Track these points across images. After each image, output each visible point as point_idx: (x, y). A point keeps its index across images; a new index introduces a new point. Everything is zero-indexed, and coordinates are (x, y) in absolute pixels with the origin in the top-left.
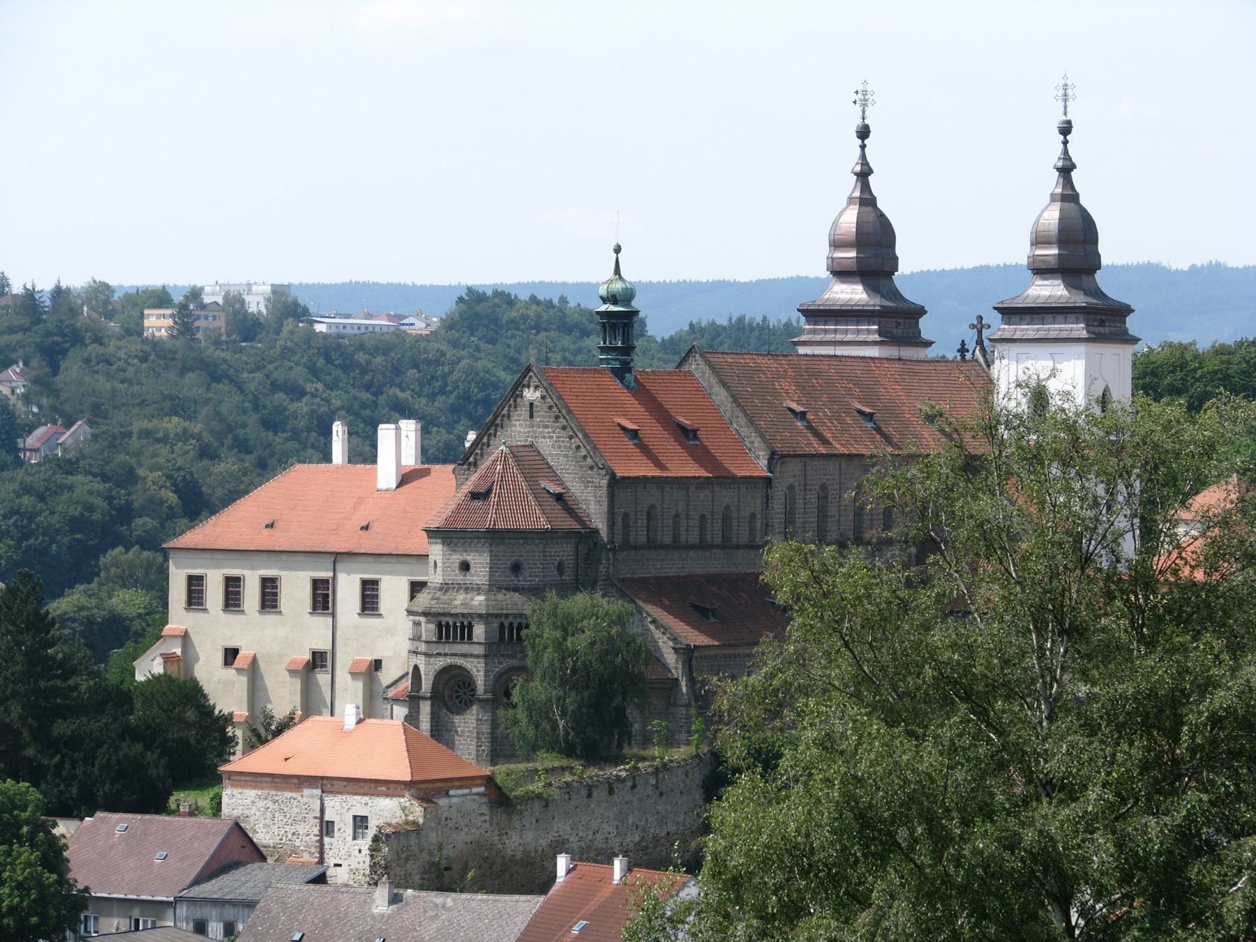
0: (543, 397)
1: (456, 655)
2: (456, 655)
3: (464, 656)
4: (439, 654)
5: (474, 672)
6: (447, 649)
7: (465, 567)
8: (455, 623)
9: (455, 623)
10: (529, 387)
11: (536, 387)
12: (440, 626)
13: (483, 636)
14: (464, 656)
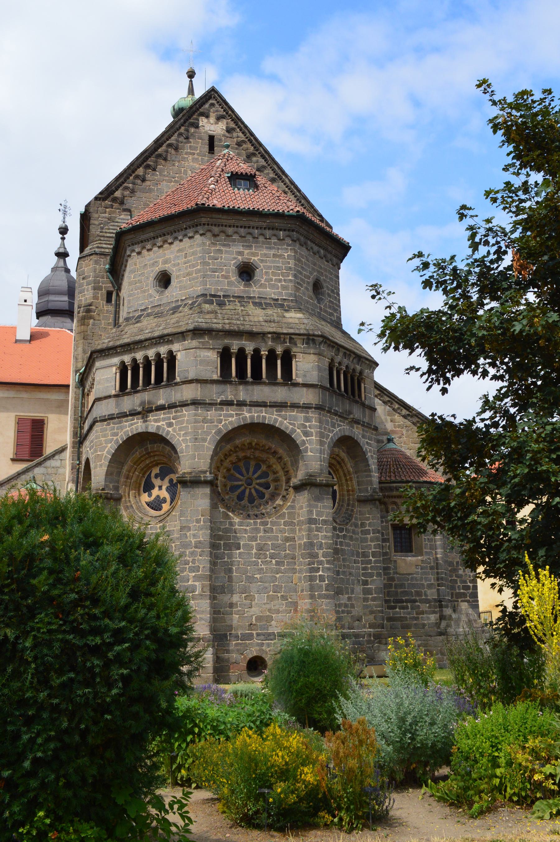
0: (229, 130)
1: (263, 405)
2: (263, 405)
3: (281, 406)
4: (229, 403)
5: (298, 436)
6: (243, 393)
7: (246, 272)
8: (257, 351)
9: (257, 351)
10: (207, 117)
11: (219, 118)
12: (225, 355)
13: (315, 373)
14: (281, 406)
